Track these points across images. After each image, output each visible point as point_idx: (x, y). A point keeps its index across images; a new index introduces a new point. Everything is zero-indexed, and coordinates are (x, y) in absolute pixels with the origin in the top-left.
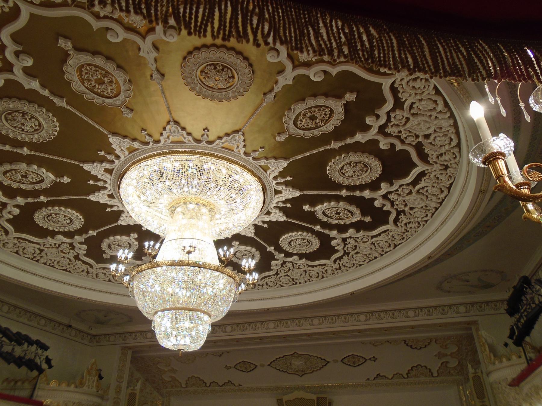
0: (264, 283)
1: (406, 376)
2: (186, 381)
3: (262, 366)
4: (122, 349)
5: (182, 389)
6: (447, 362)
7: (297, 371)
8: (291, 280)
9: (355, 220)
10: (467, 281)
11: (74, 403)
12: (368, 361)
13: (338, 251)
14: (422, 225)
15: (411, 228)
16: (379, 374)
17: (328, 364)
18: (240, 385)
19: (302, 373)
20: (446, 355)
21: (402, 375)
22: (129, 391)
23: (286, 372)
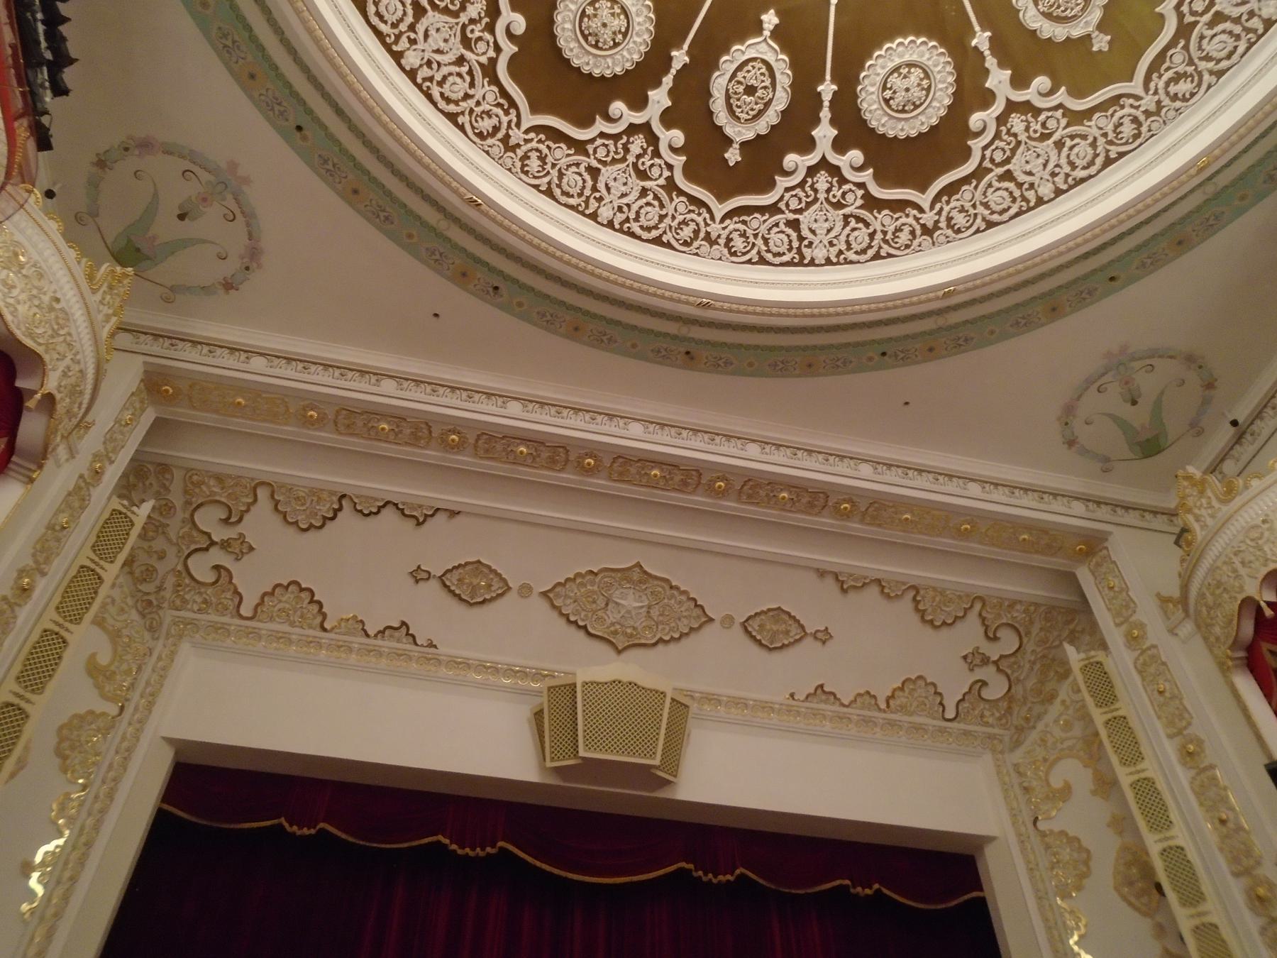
0: (724, 234)
1: (883, 706)
2: (265, 594)
3: (525, 590)
4: (142, 381)
5: (237, 621)
6: (984, 684)
7: (615, 633)
8: (795, 244)
9: (1077, 32)
10: (1134, 403)
11: (58, 300)
12: (809, 640)
13: (967, 153)
14: (1204, 86)
15: (1175, 98)
16: (822, 686)
17: (707, 629)
18: (431, 645)
19: (620, 642)
20: (985, 661)
21: (874, 697)
22: (116, 504)
23: (585, 628)
